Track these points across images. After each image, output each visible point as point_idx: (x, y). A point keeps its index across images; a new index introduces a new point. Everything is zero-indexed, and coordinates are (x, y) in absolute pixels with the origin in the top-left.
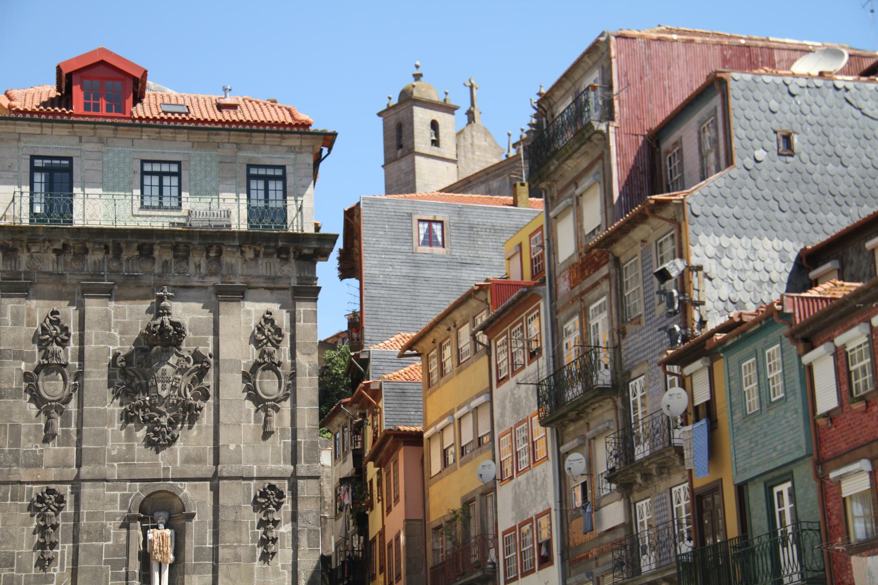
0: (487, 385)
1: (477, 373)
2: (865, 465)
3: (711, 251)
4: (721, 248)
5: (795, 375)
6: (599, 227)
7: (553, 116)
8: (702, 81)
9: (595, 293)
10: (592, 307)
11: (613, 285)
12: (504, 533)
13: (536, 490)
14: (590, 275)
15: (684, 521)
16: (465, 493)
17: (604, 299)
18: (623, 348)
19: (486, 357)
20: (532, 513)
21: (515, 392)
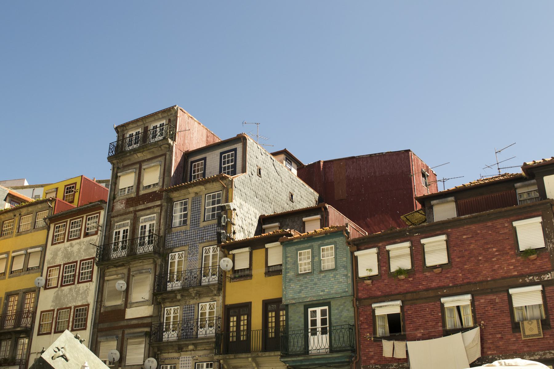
0: (44, 243)
1: (39, 237)
2: (399, 303)
3: (238, 205)
4: (241, 204)
5: (346, 260)
6: (157, 184)
7: (124, 135)
8: (234, 135)
9: (148, 212)
10: (141, 218)
11: (164, 210)
12: (42, 312)
13: (77, 294)
14: (144, 204)
15: (199, 320)
16: (8, 291)
17: (155, 215)
18: (167, 238)
19: (46, 231)
20: (72, 305)
21: (69, 249)
